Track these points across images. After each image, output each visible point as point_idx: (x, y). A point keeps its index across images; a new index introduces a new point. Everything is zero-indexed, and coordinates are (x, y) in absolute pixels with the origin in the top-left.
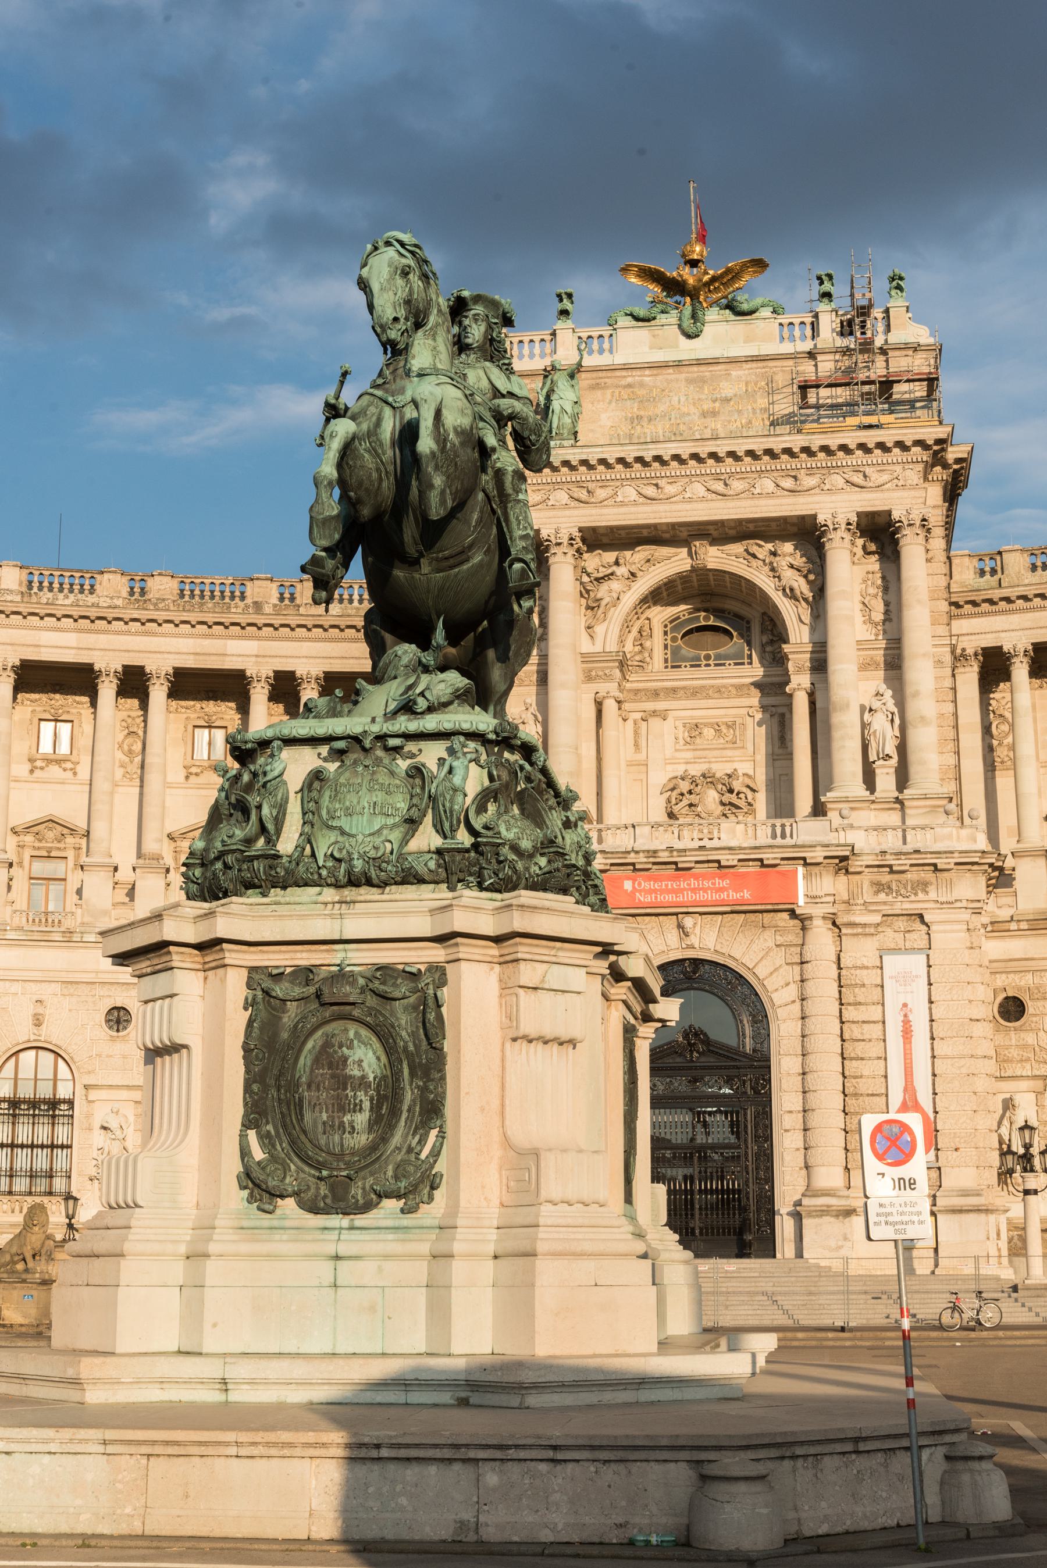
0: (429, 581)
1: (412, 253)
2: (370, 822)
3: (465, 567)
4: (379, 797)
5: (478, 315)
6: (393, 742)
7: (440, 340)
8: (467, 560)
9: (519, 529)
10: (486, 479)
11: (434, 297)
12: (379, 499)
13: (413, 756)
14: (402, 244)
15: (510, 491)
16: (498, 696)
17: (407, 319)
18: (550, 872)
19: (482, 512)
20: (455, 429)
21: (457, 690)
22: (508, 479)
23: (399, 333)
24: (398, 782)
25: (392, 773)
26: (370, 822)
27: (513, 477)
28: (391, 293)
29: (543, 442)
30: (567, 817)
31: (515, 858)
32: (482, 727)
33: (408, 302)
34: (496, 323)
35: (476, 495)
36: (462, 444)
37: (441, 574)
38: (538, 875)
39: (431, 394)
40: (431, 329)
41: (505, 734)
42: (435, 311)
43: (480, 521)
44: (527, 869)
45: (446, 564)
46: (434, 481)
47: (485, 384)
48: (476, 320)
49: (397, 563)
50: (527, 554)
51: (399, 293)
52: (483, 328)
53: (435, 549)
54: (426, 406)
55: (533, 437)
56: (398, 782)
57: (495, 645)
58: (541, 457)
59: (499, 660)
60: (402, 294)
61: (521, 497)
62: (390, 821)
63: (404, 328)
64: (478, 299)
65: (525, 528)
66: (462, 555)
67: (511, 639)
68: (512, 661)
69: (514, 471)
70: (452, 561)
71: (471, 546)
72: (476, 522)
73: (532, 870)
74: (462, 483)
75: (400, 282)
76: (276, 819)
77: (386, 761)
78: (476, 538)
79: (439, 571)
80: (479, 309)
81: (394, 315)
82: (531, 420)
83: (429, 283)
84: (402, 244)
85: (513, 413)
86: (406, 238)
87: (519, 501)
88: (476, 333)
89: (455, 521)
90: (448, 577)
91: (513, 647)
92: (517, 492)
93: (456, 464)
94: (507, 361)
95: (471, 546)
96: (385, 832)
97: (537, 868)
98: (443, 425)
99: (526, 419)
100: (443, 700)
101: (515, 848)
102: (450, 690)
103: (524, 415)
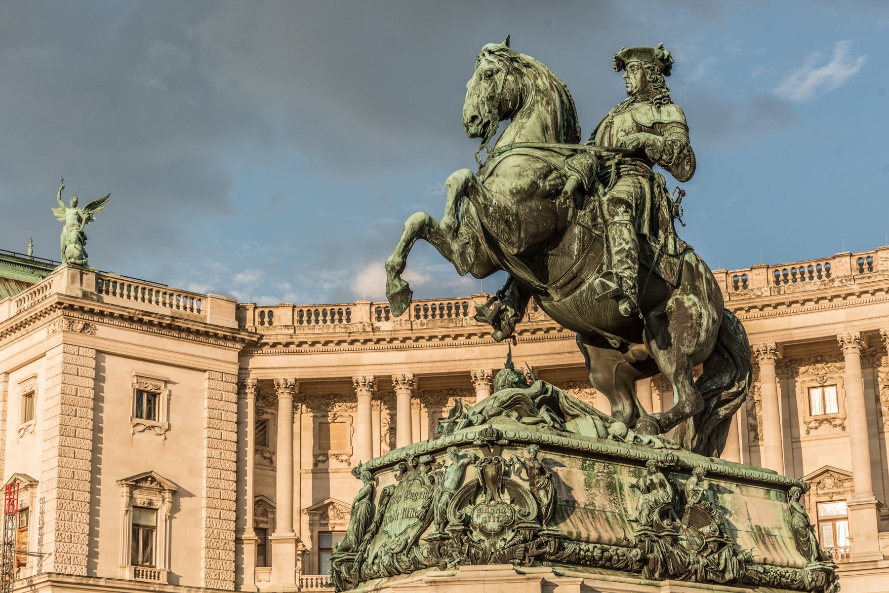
0: (564, 304)
1: (500, 55)
2: (400, 524)
3: (584, 287)
4: (409, 504)
5: (633, 66)
6: (424, 459)
7: (534, 115)
8: (583, 282)
9: (615, 246)
10: (584, 216)
11: (529, 81)
12: (485, 259)
13: (440, 466)
14: (491, 52)
15: (607, 217)
16: (672, 378)
17: (490, 112)
18: (514, 545)
19: (582, 240)
20: (511, 192)
21: (503, 403)
22: (605, 207)
23: (480, 127)
24: (423, 490)
25: (422, 483)
26: (400, 524)
27: (608, 205)
28: (475, 97)
29: (679, 157)
30: (651, 480)
31: (483, 538)
32: (470, 436)
33: (491, 98)
34: (649, 68)
35: (572, 230)
36: (519, 202)
37: (569, 298)
38: (503, 549)
39: (454, 179)
40: (529, 108)
41: (486, 439)
42: (533, 93)
43: (582, 249)
44: (493, 545)
45: (566, 289)
46: (453, 248)
47: (629, 123)
48: (633, 70)
49: (541, 297)
50: (623, 265)
51: (483, 94)
52: (638, 76)
53: (551, 281)
54: (450, 190)
55: (664, 157)
56: (423, 490)
57: (654, 337)
58: (683, 168)
59: (660, 348)
60: (484, 94)
61: (617, 219)
62: (412, 522)
63: (485, 120)
64: (629, 53)
65: (621, 244)
66: (574, 281)
67: (670, 329)
68: (675, 346)
69: (609, 200)
70: (570, 286)
71: (580, 270)
72: (579, 251)
73: (498, 546)
74: (526, 231)
75: (484, 84)
76: (357, 530)
77: (422, 475)
78: (581, 264)
79: (566, 295)
80: (634, 61)
81: (476, 113)
82: (659, 144)
83: (522, 74)
84: (491, 52)
85: (639, 144)
86: (491, 46)
87: (615, 223)
88: (634, 80)
89: (551, 258)
90: (575, 298)
91: (672, 335)
92: (613, 216)
93: (507, 222)
94: (658, 97)
95: (580, 270)
96: (409, 531)
97: (502, 544)
98: (485, 196)
99: (654, 145)
100: (490, 413)
101: (483, 530)
102: (496, 405)
103: (651, 142)
